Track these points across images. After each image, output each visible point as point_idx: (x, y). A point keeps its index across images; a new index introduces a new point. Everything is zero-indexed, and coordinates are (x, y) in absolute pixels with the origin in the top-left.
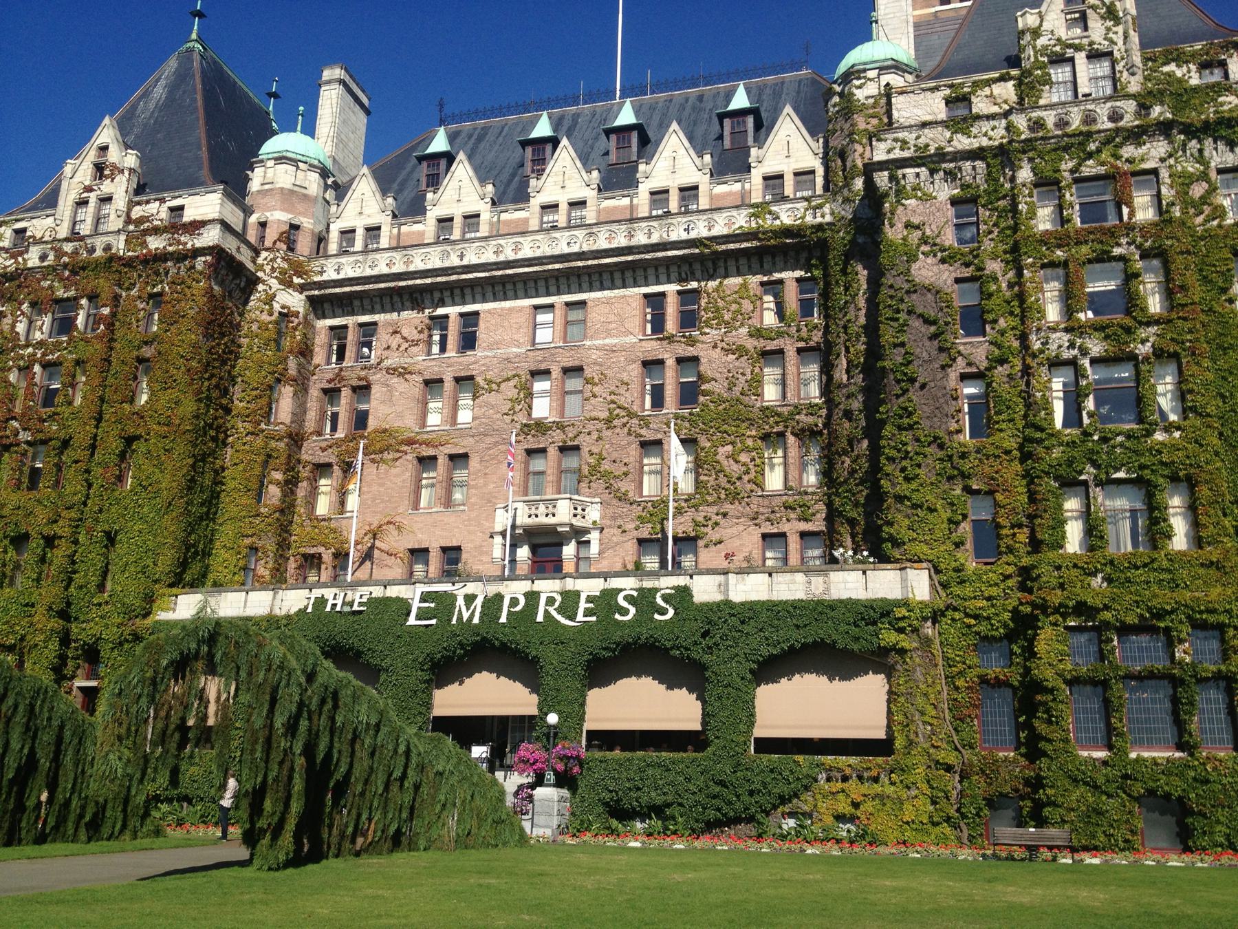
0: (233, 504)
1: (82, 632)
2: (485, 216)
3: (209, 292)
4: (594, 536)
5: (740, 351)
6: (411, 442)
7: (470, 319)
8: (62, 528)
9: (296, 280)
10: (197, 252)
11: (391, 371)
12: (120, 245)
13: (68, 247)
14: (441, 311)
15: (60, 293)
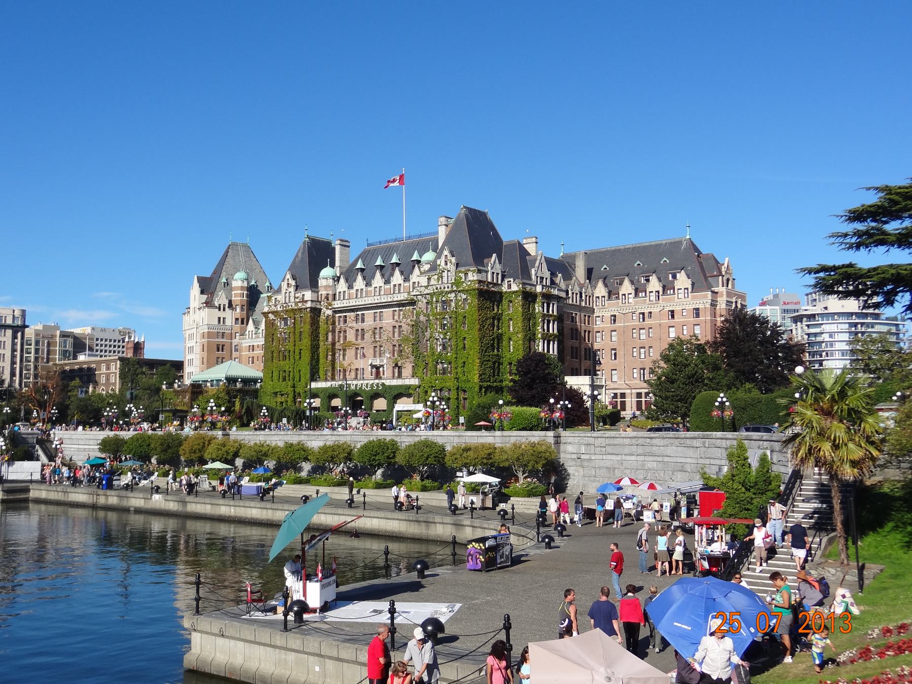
0: (322, 361)
1: (297, 390)
2: (364, 290)
3: (311, 316)
4: (385, 366)
5: (409, 325)
6: (354, 344)
7: (363, 315)
8: (291, 369)
9: (330, 307)
10: (307, 308)
11: (350, 327)
12: (294, 307)
13: (285, 305)
14: (358, 313)
15: (285, 316)
